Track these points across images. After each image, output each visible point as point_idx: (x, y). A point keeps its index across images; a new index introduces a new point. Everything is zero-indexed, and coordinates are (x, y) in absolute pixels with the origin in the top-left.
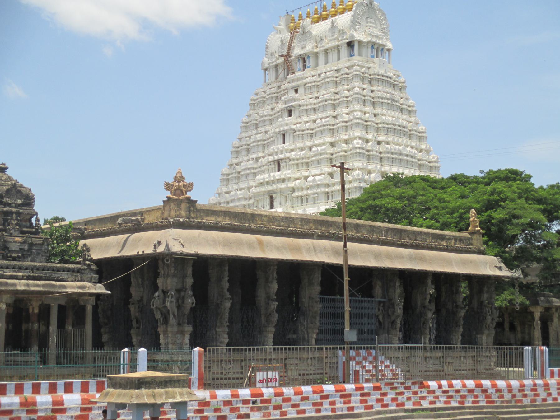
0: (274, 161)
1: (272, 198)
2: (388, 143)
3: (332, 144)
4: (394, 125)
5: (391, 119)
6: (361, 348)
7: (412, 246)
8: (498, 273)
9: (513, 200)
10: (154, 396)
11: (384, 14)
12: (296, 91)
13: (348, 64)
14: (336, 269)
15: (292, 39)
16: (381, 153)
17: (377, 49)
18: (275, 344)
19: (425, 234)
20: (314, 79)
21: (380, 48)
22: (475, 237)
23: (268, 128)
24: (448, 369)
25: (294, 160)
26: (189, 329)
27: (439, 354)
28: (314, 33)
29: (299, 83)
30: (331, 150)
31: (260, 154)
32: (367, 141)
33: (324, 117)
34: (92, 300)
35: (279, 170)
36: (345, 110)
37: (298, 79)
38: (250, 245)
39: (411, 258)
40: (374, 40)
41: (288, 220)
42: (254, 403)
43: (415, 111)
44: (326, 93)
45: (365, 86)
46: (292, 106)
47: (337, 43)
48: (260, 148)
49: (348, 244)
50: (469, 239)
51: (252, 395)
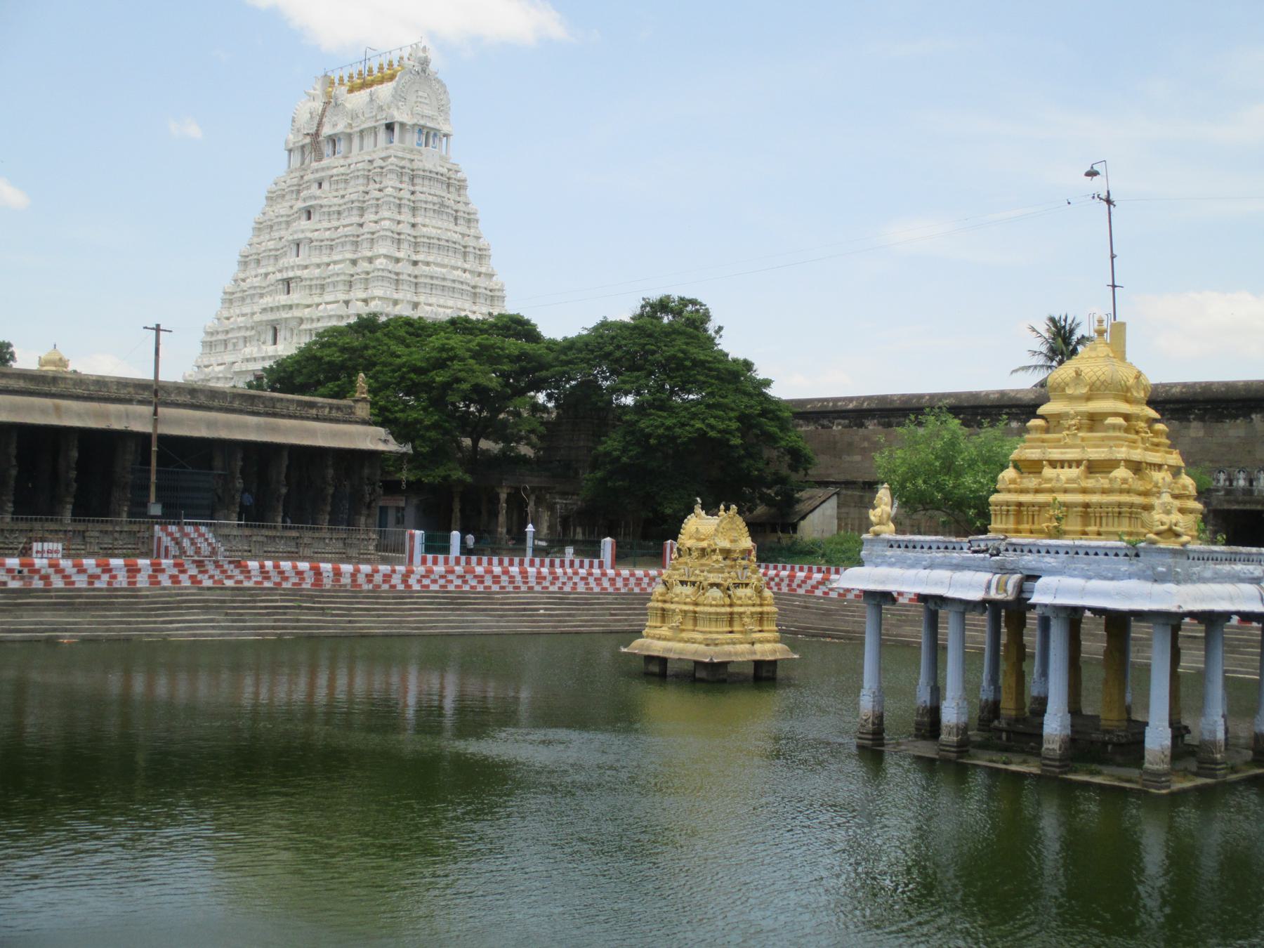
0: (283, 280)
1: (275, 330)
2: (428, 264)
5: (434, 231)
6: (200, 524)
7: (267, 414)
8: (381, 447)
9: (462, 359)
11: (443, 86)
13: (384, 155)
14: (145, 438)
15: (324, 110)
16: (416, 277)
17: (428, 134)
18: (73, 514)
19: (288, 400)
20: (342, 170)
22: (359, 405)
23: (283, 233)
27: (294, 534)
28: (349, 106)
29: (323, 174)
31: (271, 269)
32: (398, 260)
35: (288, 293)
36: (373, 217)
37: (323, 169)
38: (43, 411)
40: (422, 122)
43: (477, 221)
44: (354, 191)
47: (373, 124)
48: (272, 261)
49: (160, 410)
50: (350, 407)
51: (22, 565)
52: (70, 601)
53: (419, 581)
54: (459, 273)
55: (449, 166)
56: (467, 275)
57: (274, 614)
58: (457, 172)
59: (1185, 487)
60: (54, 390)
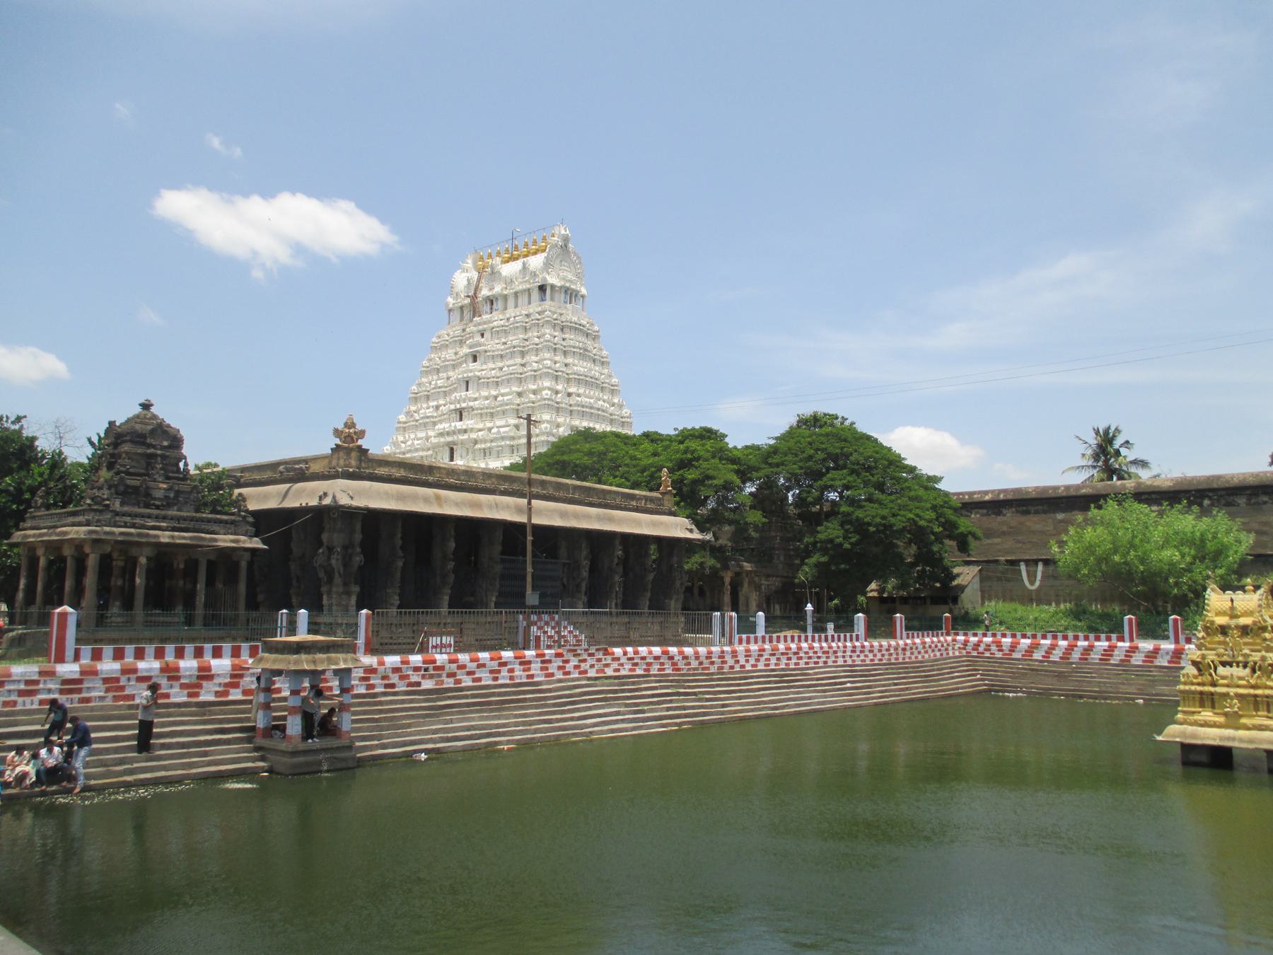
1: (452, 450)
2: (579, 395)
3: (520, 394)
8: (689, 535)
10: (314, 662)
12: (482, 335)
18: (450, 606)
22: (667, 497)
23: (451, 373)
24: (634, 635)
26: (356, 589)
30: (518, 401)
31: (441, 402)
32: (557, 392)
33: (512, 365)
34: (247, 556)
37: (485, 323)
38: (426, 500)
39: (599, 518)
41: (469, 473)
42: (426, 670)
44: (515, 339)
51: (424, 662)
52: (487, 701)
60: (431, 479)
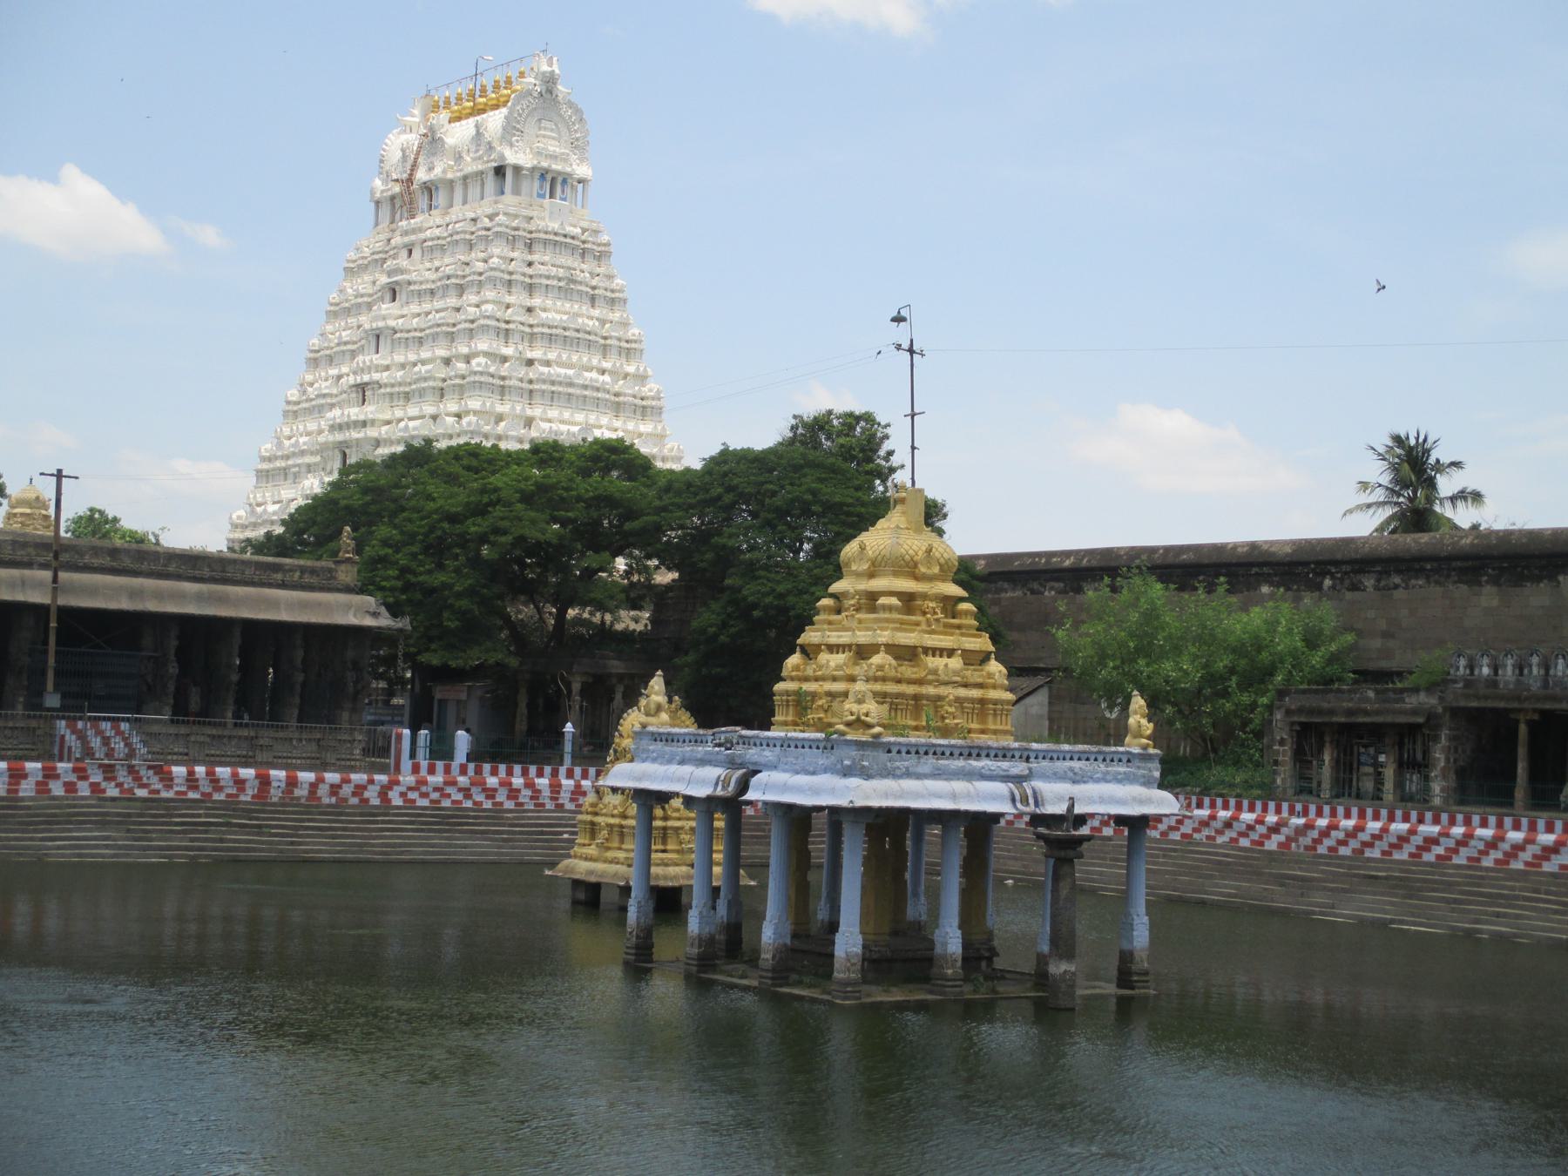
0: (357, 386)
2: (548, 363)
3: (447, 362)
4: (565, 329)
5: (558, 317)
8: (369, 622)
9: (508, 504)
11: (578, 111)
14: (40, 611)
16: (531, 382)
17: (553, 182)
20: (437, 232)
21: (560, 179)
22: (343, 567)
24: (330, 757)
25: (386, 385)
29: (413, 237)
30: (442, 373)
31: (345, 369)
32: (505, 359)
33: (439, 310)
37: (414, 231)
39: (199, 598)
40: (545, 164)
43: (625, 301)
44: (448, 263)
45: (515, 255)
46: (396, 283)
47: (480, 167)
50: (330, 570)
53: (403, 795)
54: (594, 375)
55: (585, 225)
56: (607, 378)
57: (192, 832)
58: (596, 232)
59: (990, 675)
